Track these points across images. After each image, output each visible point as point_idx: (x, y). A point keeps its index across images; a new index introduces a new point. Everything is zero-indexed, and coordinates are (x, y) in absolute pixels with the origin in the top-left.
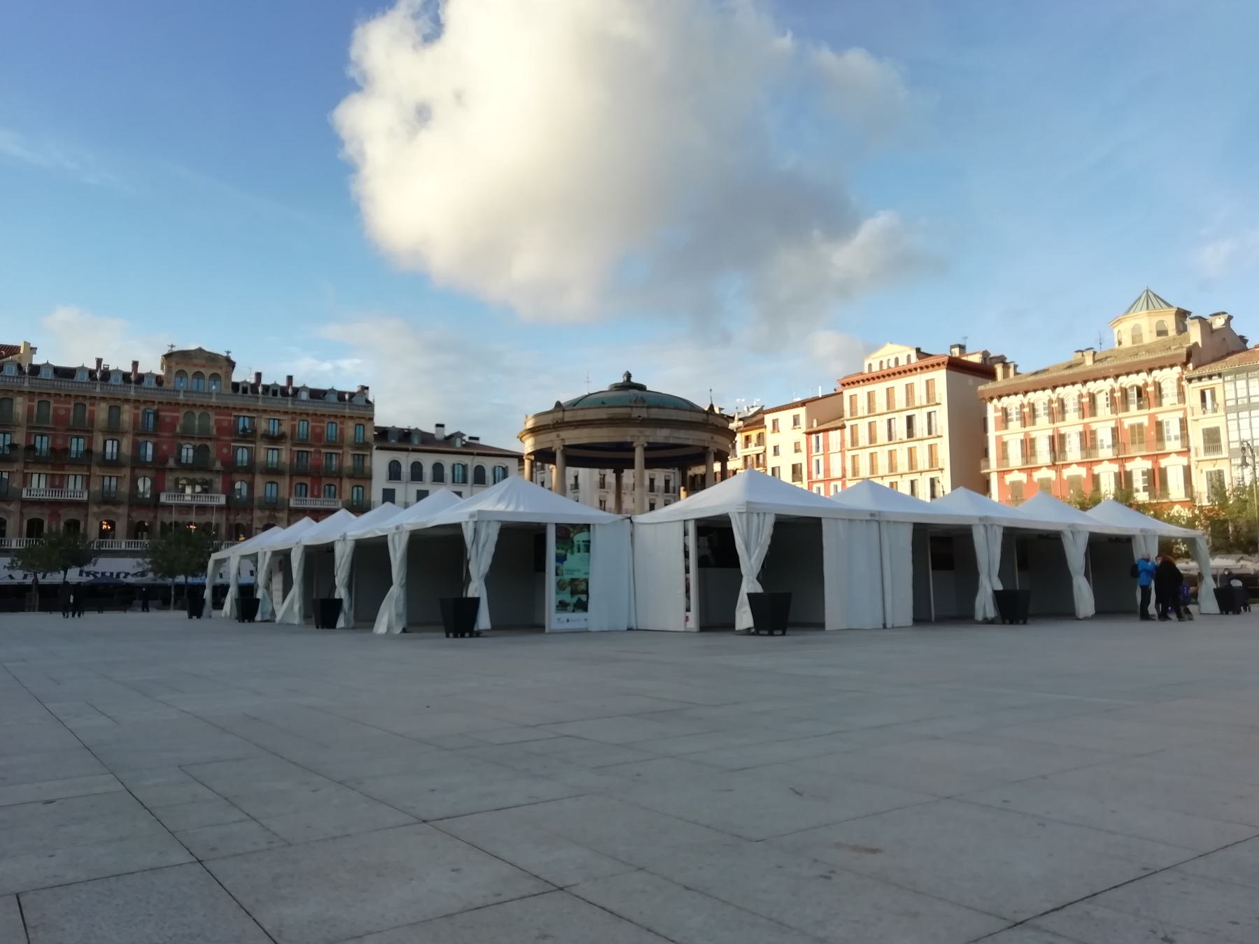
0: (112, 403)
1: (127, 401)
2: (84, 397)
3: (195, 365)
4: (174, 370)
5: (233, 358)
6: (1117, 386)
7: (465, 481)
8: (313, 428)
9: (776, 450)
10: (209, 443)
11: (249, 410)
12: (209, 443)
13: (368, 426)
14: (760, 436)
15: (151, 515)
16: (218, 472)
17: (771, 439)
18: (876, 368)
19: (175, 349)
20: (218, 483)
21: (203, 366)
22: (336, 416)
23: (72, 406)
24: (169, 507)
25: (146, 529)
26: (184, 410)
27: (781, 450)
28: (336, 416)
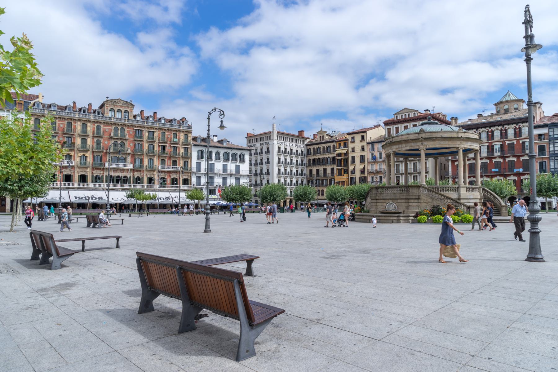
0: (83, 122)
1: (90, 122)
2: (71, 119)
3: (118, 106)
4: (109, 108)
5: (132, 103)
6: (503, 129)
7: (228, 160)
8: (168, 135)
9: (353, 150)
10: (124, 141)
11: (141, 127)
12: (124, 141)
13: (189, 135)
14: (345, 144)
15: (102, 172)
16: (129, 154)
17: (350, 146)
18: (399, 117)
19: (109, 99)
20: (129, 159)
21: (121, 107)
22: (177, 131)
23: (66, 123)
24: (109, 169)
25: (99, 179)
26: (113, 127)
27: (355, 149)
28: (177, 131)
